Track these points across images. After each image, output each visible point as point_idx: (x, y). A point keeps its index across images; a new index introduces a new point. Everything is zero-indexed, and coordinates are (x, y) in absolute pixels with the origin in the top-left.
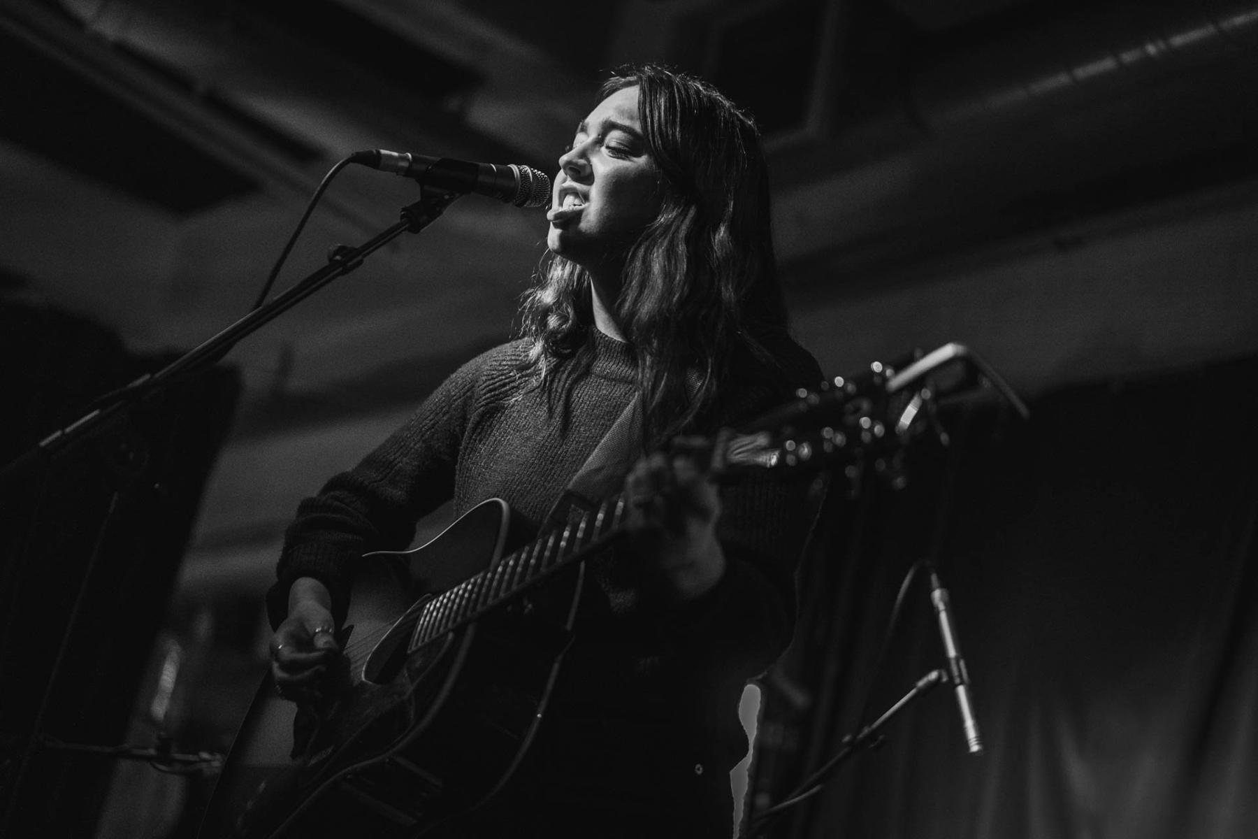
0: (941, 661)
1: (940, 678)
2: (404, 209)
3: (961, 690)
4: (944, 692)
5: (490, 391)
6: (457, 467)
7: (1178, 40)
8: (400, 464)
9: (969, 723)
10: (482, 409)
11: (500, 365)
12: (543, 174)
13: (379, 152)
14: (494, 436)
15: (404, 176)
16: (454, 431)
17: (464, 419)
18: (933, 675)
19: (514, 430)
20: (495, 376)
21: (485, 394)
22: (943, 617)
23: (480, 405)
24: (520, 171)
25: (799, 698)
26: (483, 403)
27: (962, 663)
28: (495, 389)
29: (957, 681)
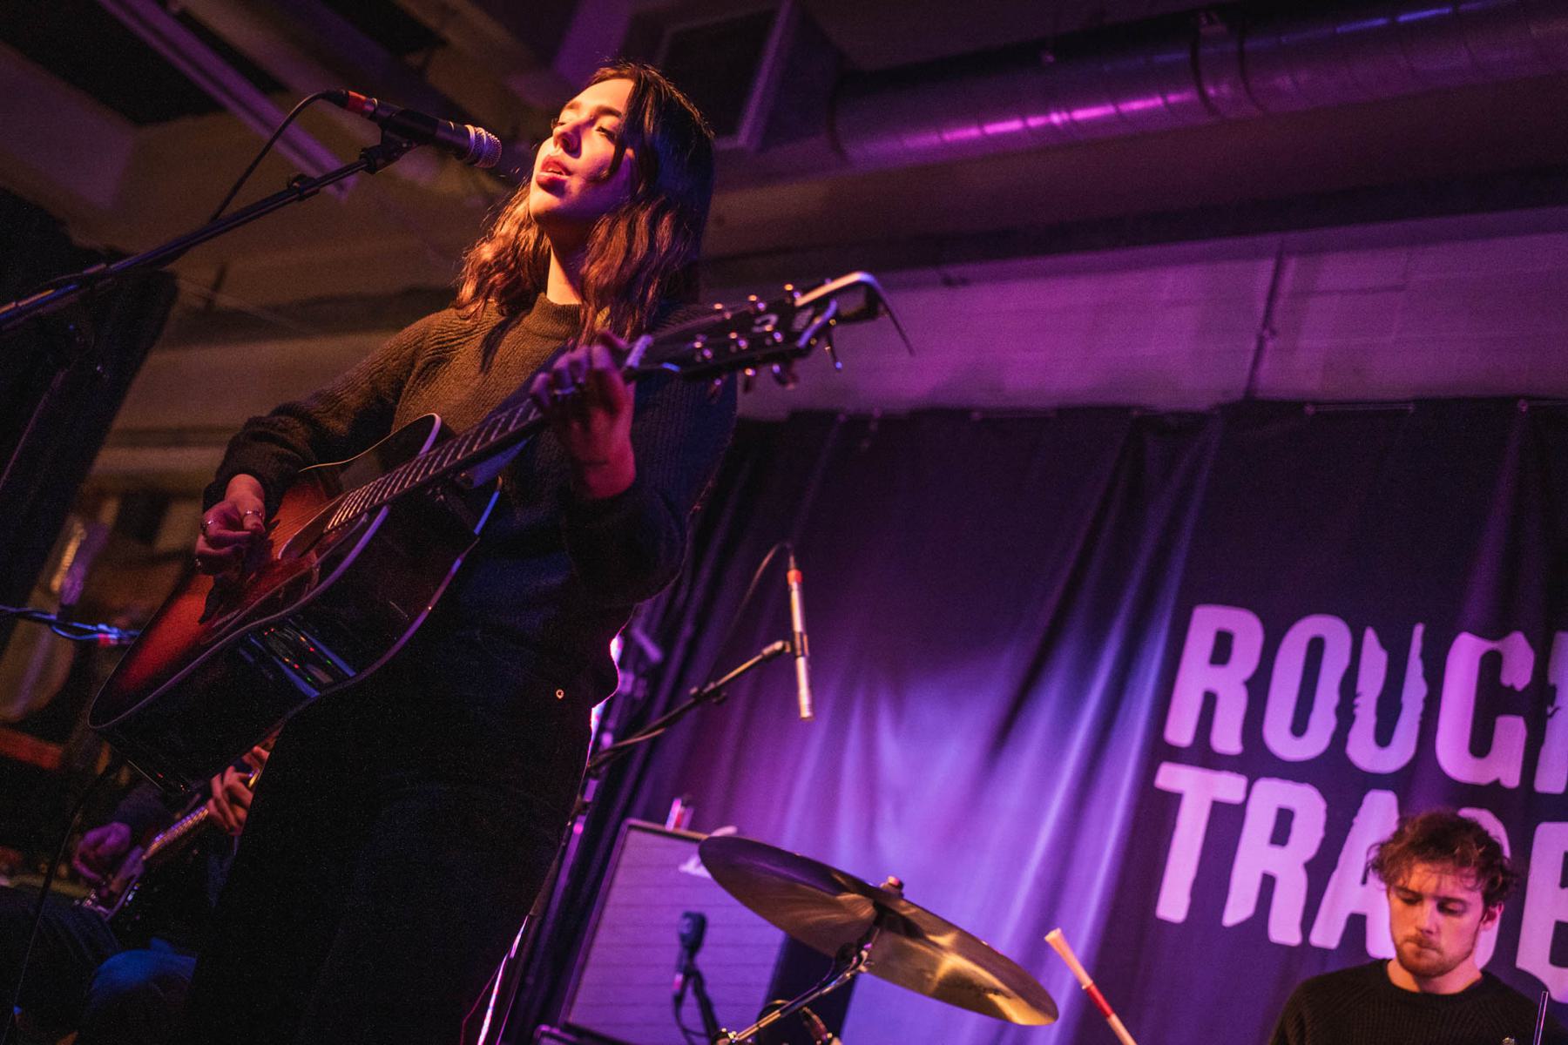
0: (786, 632)
1: (784, 647)
3: (801, 663)
4: (784, 663)
5: (439, 343)
6: (398, 407)
7: (1080, 115)
8: (346, 400)
11: (451, 322)
16: (401, 376)
17: (413, 365)
18: (778, 645)
21: (432, 345)
22: (795, 597)
26: (431, 353)
27: (805, 638)
28: (444, 342)
29: (799, 653)
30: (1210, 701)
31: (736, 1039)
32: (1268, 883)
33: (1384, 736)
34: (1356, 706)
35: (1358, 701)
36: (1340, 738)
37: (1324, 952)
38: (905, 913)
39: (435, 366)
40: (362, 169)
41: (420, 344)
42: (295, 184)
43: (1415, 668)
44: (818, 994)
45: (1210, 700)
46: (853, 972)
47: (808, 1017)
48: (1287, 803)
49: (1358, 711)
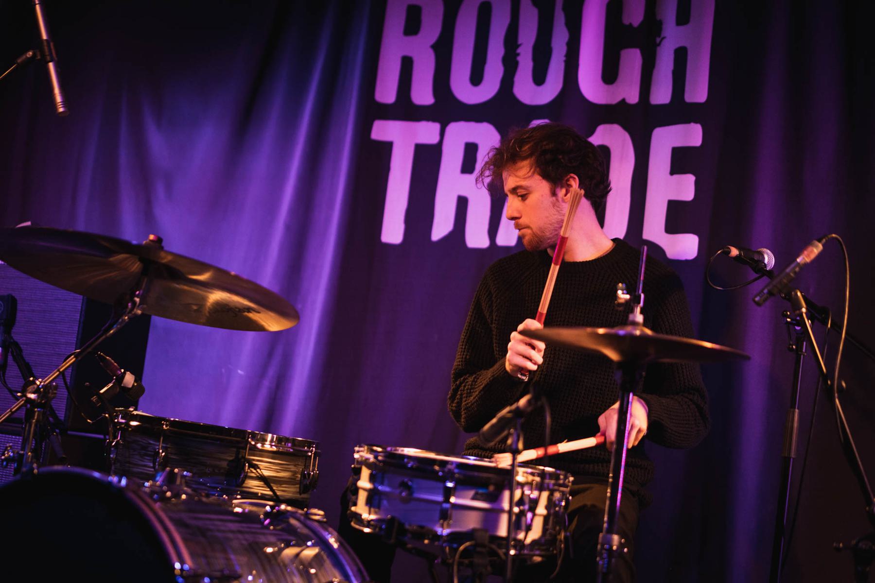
30: (407, 65)
31: (42, 384)
32: (462, 203)
33: (539, 78)
34: (518, 54)
35: (519, 51)
36: (507, 82)
37: (507, 249)
38: (164, 261)
43: (560, 19)
44: (104, 337)
45: (407, 65)
46: (130, 315)
47: (102, 359)
48: (471, 139)
49: (519, 59)
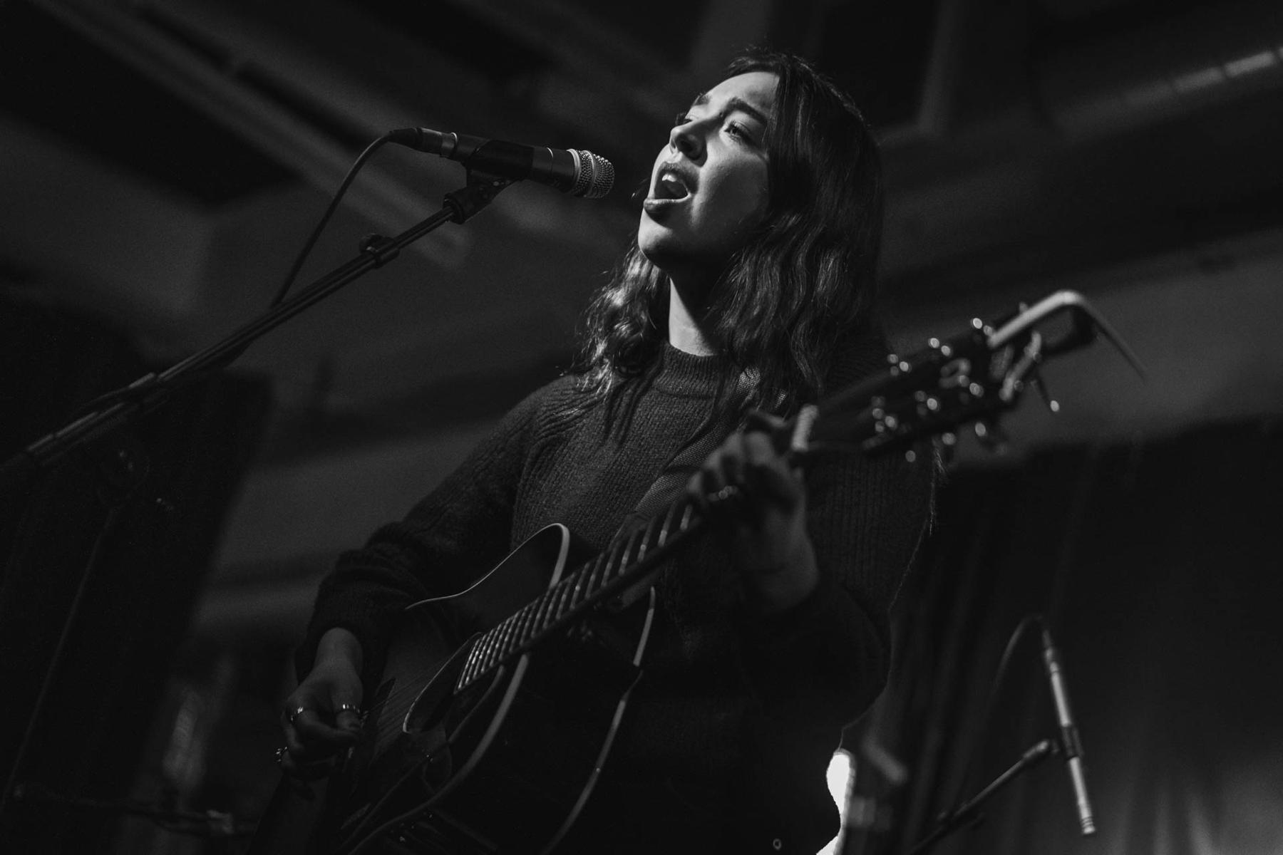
1: (1049, 749)
2: (447, 196)
3: (1075, 764)
6: (515, 507)
9: (1082, 801)
10: (542, 441)
11: (562, 394)
12: (606, 161)
13: (420, 131)
14: (556, 470)
15: (448, 158)
18: (1042, 746)
19: (578, 464)
20: (556, 406)
21: (545, 425)
22: (1056, 681)
23: (539, 437)
24: (581, 157)
25: (894, 771)
26: (543, 434)
27: (1075, 733)
29: (1070, 752)
39: (550, 450)
40: (447, 220)
41: (526, 427)
42: (369, 248)
